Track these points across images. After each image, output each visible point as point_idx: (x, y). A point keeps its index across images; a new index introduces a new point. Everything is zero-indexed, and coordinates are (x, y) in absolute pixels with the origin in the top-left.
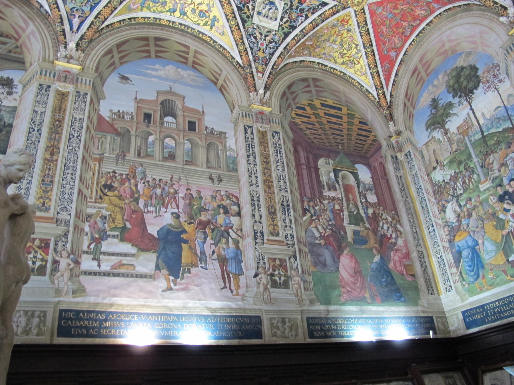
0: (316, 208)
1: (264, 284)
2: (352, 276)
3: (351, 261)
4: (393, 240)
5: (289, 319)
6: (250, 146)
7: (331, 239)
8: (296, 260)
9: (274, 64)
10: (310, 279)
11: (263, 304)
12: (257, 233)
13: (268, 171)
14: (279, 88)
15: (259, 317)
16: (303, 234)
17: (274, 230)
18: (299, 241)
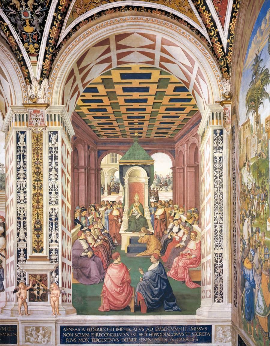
0: (89, 218)
1: (22, 298)
2: (118, 287)
3: (120, 271)
4: (183, 244)
5: (43, 327)
6: (21, 157)
7: (101, 250)
8: (57, 274)
9: (49, 38)
10: (70, 291)
11: (20, 316)
12: (20, 251)
13: (39, 182)
14: (66, 66)
15: (16, 327)
16: (70, 247)
17: (38, 246)
18: (64, 256)
